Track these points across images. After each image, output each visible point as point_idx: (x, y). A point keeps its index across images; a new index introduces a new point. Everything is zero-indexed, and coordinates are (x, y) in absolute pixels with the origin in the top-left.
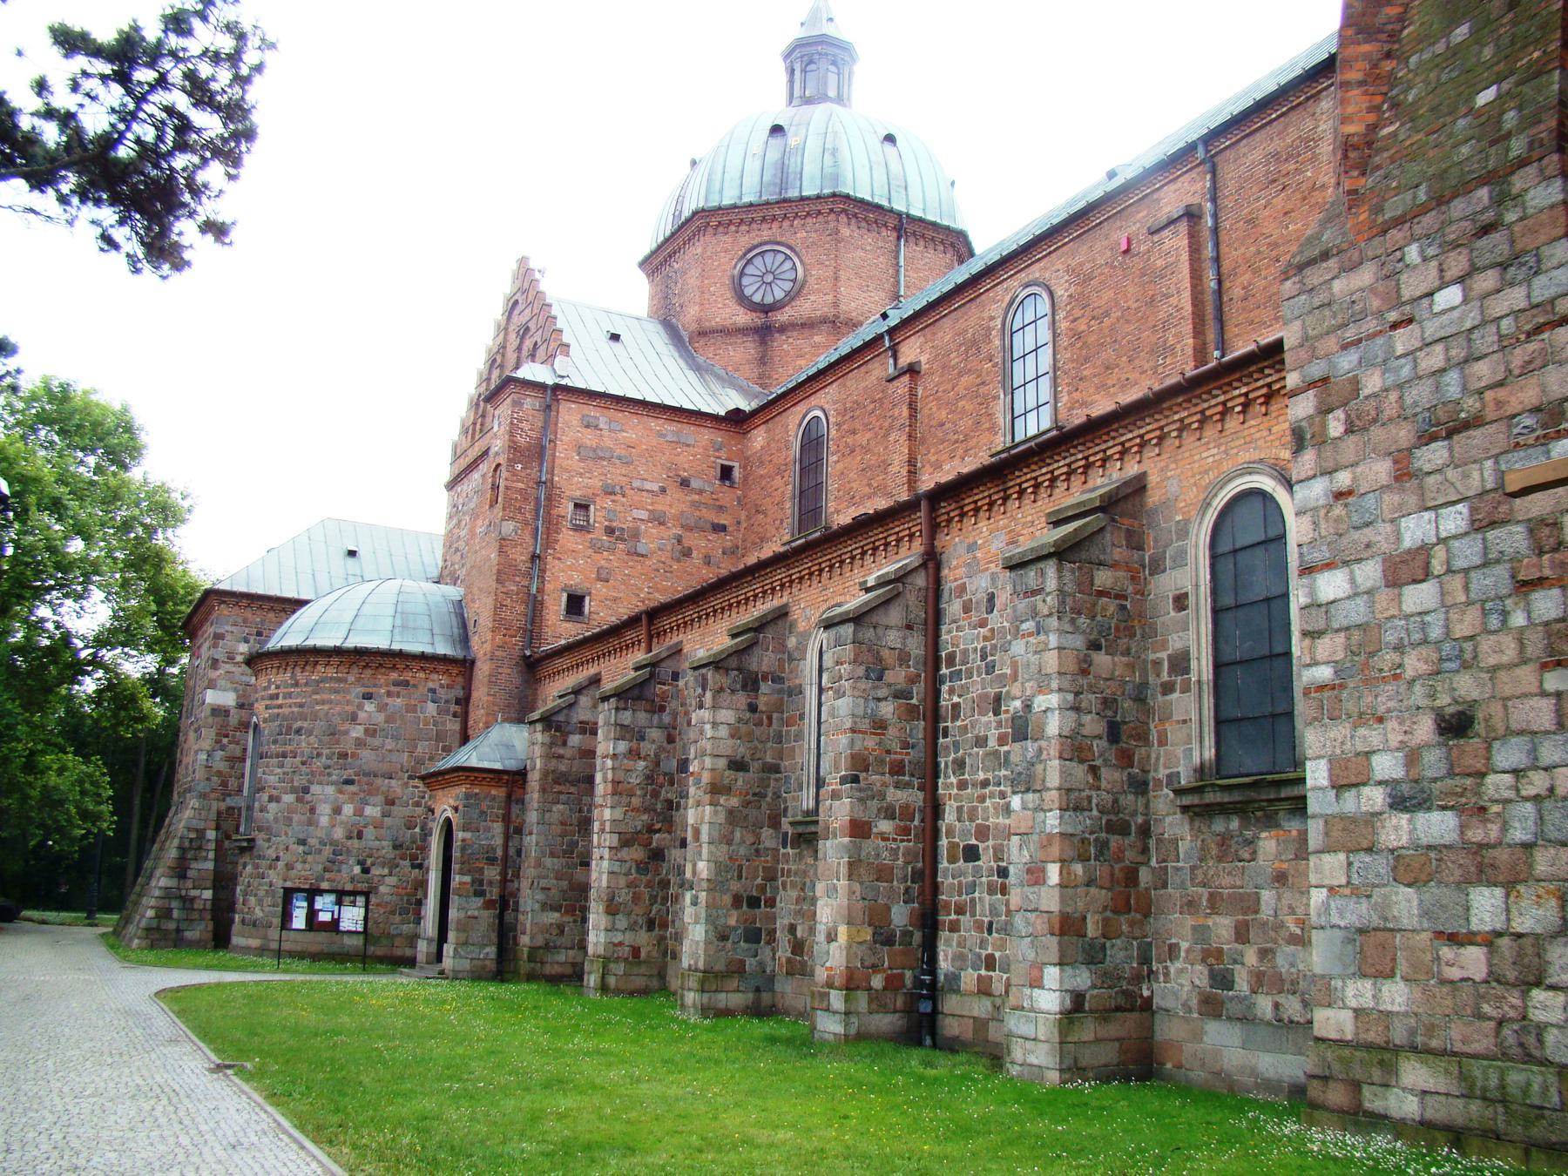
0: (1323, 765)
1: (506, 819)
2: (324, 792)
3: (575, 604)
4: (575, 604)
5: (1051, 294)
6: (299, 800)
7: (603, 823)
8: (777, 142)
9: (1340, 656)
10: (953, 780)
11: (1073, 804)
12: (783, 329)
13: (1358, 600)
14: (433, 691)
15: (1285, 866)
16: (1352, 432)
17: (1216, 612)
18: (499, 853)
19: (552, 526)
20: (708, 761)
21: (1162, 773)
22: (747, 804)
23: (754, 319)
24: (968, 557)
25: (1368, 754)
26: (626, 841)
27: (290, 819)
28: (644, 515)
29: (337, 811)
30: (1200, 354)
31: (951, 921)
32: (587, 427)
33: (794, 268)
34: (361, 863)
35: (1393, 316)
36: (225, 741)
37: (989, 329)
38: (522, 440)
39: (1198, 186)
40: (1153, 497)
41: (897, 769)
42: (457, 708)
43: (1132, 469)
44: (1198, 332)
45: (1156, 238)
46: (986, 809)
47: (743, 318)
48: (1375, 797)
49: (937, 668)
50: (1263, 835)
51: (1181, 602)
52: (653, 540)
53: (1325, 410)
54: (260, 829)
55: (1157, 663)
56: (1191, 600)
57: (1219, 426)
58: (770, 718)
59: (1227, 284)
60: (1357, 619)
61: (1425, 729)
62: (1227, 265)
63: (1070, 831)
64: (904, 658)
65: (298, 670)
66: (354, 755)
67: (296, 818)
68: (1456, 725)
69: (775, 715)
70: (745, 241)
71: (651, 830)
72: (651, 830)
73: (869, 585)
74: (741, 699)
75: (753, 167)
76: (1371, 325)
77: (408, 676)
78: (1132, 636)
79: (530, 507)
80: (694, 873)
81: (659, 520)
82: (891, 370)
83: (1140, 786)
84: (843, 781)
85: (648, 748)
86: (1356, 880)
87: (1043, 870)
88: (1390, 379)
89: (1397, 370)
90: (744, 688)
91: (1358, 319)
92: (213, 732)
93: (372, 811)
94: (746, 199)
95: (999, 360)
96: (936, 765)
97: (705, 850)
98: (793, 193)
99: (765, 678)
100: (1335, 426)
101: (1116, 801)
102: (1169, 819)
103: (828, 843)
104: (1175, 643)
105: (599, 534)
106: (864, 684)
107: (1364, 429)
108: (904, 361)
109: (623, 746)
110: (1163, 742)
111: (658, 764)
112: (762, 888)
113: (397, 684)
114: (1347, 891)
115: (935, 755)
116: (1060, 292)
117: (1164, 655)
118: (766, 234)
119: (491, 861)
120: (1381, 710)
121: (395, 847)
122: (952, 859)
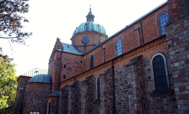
0: (178, 88)
1: (57, 102)
3: (64, 77)
4: (64, 77)
5: (121, 39)
6: (31, 100)
7: (70, 102)
9: (179, 73)
10: (117, 94)
11: (137, 96)
12: (87, 46)
13: (181, 66)
14: (47, 87)
15: (167, 103)
16: (178, 45)
17: (154, 71)
18: (56, 106)
19: (62, 68)
20: (84, 94)
21: (148, 92)
22: (89, 99)
23: (84, 45)
24: (118, 67)
25: (185, 86)
26: (73, 104)
27: (30, 103)
28: (72, 66)
29: (36, 102)
30: (141, 44)
31: (118, 112)
32: (66, 56)
33: (88, 39)
34: (39, 108)
35: (183, 29)
36: (22, 94)
37: (114, 44)
39: (139, 26)
40: (144, 58)
41: (110, 93)
42: (50, 89)
43: (140, 54)
44: (140, 42)
45: (135, 31)
46: (122, 98)
47: (83, 44)
49: (114, 81)
50: (164, 99)
51: (149, 70)
52: (73, 69)
53: (173, 42)
54: (26, 104)
55: (146, 78)
56: (151, 69)
57: (153, 48)
58: (91, 88)
59: (144, 36)
60: (181, 68)
62: (144, 34)
63: (137, 99)
64: (110, 80)
65: (31, 85)
66: (38, 95)
67: (31, 103)
69: (92, 88)
70: (83, 36)
71: (76, 103)
72: (76, 103)
73: (105, 71)
74: (88, 86)
75: (84, 28)
76: (179, 31)
77: (45, 85)
78: (142, 74)
79: (59, 65)
80: (82, 108)
81: (74, 67)
82: (101, 49)
83: (145, 93)
84: (103, 95)
85: (75, 93)
86: (185, 103)
87: (134, 105)
88: (183, 37)
89: (184, 36)
90: (88, 85)
91: (177, 30)
92: (20, 93)
93: (40, 102)
94: (83, 31)
95: (115, 47)
96: (115, 93)
97: (84, 105)
98: (88, 31)
99: (91, 83)
100: (175, 44)
101: (142, 95)
102: (149, 98)
103: (102, 103)
104: (148, 75)
105: (67, 69)
106: (106, 83)
107: (180, 44)
108: (103, 48)
109: (72, 92)
110: (147, 87)
111: (76, 95)
112: (91, 109)
113: (43, 86)
114: (184, 105)
115: (114, 92)
116: (122, 39)
117: (147, 77)
119: (55, 107)
120: (187, 80)
121: (43, 106)
122: (117, 104)
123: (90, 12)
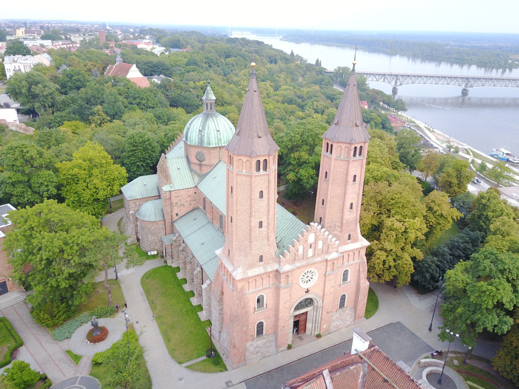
2: (149, 236)
4: (177, 215)
38: (167, 197)
52: (186, 204)
75: (197, 138)
81: (187, 202)
85: (184, 255)
94: (197, 144)
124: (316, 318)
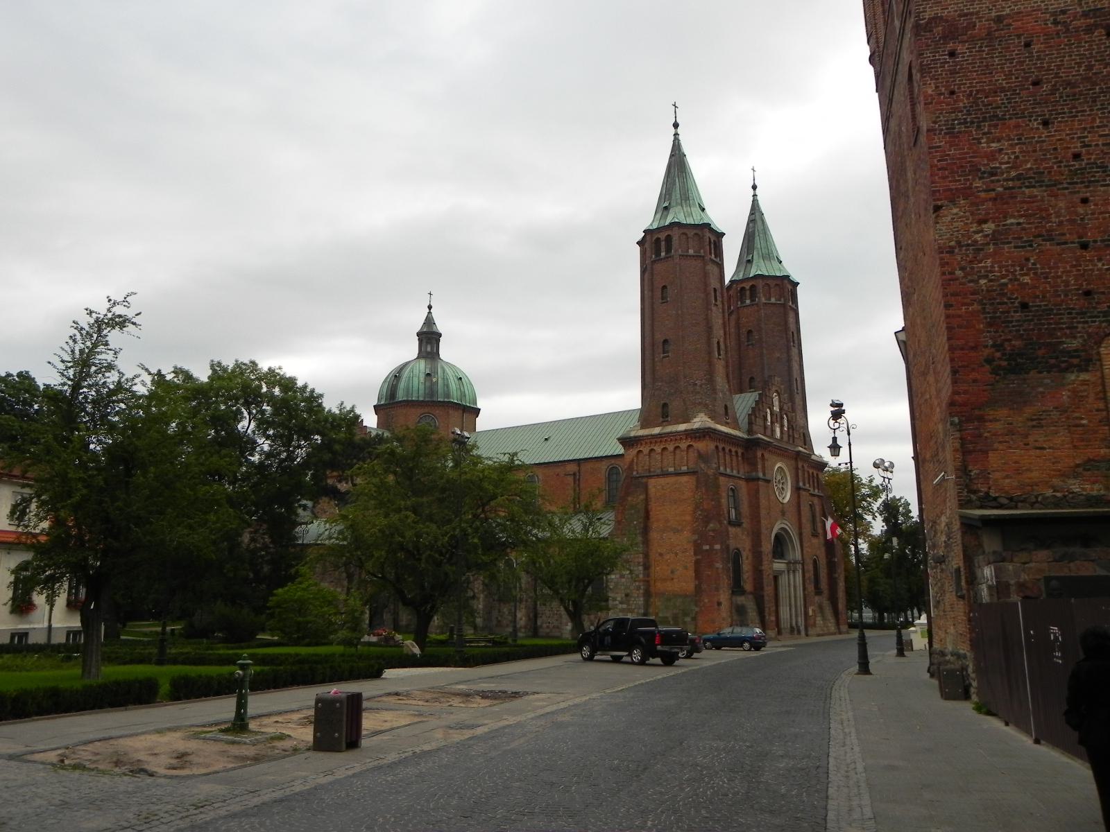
8: (428, 378)
48: (617, 602)
61: (623, 595)
62: (581, 486)
68: (627, 595)
75: (422, 387)
94: (421, 399)
98: (435, 399)
118: (426, 410)
123: (429, 321)
124: (795, 587)
